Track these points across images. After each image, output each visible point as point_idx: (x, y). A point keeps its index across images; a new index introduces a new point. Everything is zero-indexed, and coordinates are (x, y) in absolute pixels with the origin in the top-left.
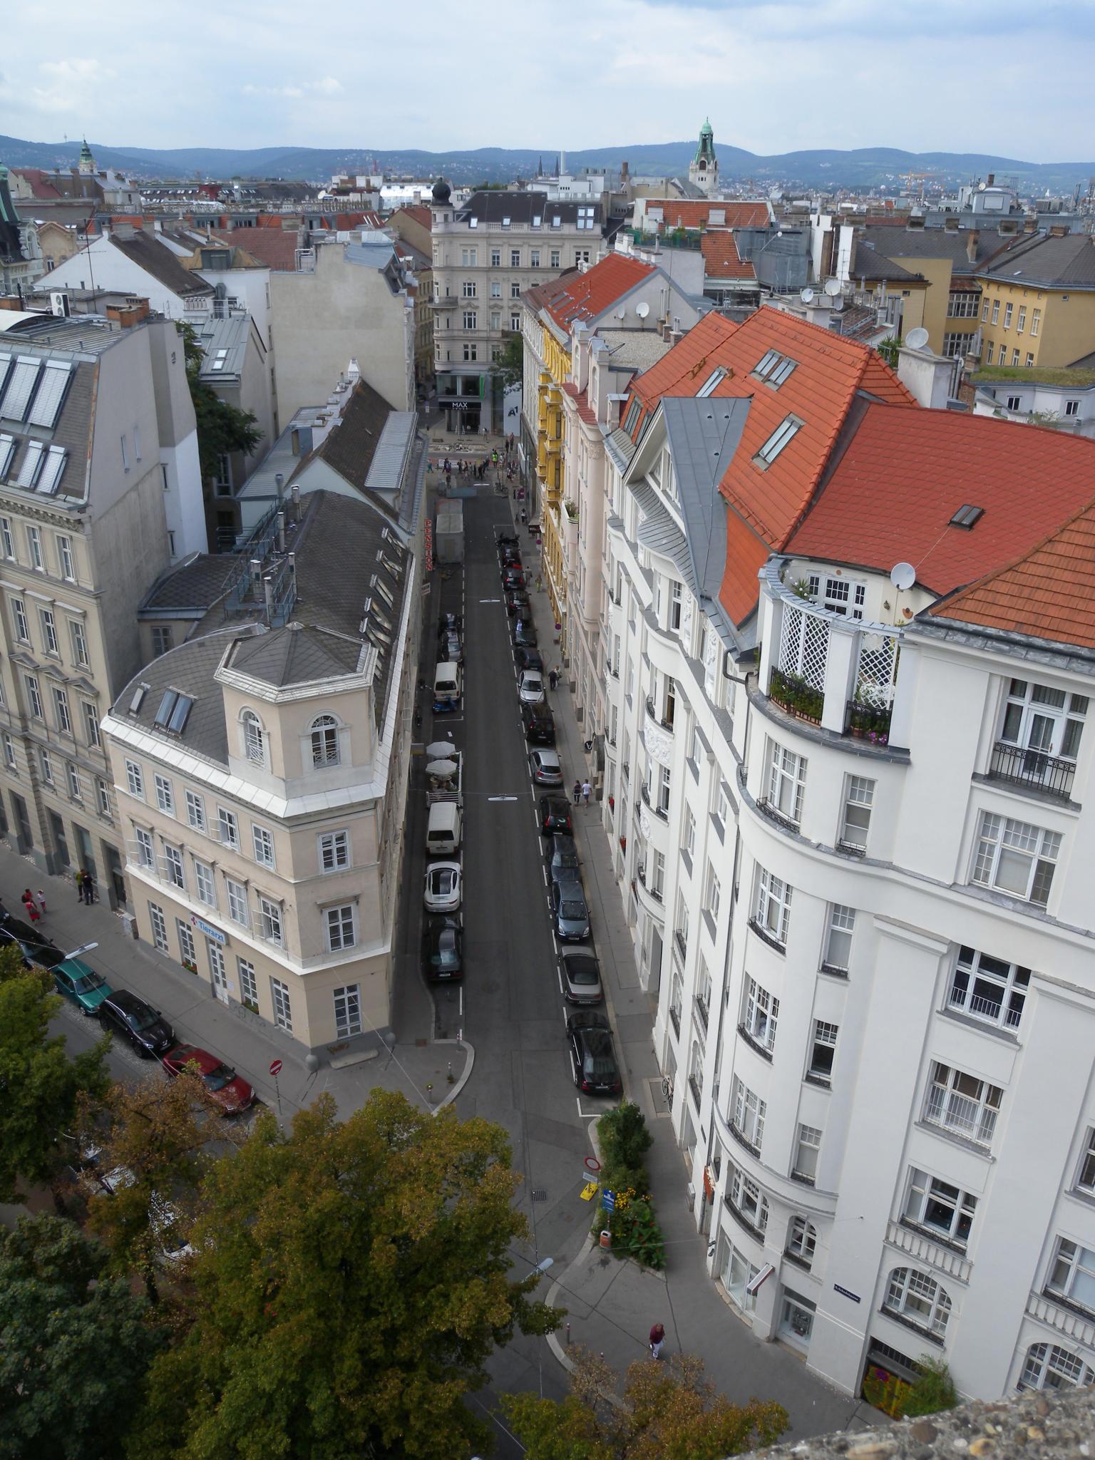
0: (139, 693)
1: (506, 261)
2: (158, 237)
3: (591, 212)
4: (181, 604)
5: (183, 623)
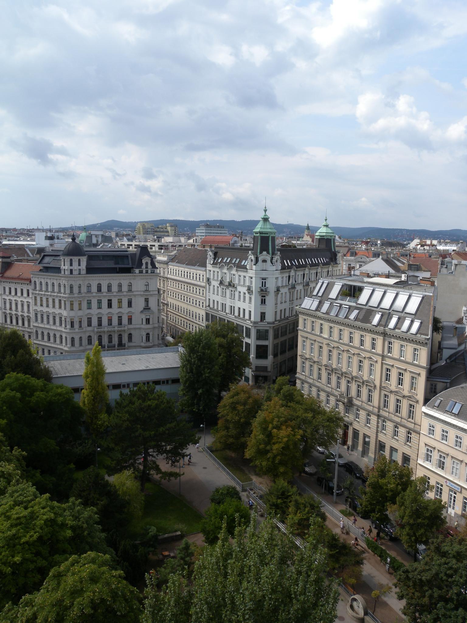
0: (439, 401)
2: (392, 259)
4: (442, 377)
5: (442, 383)
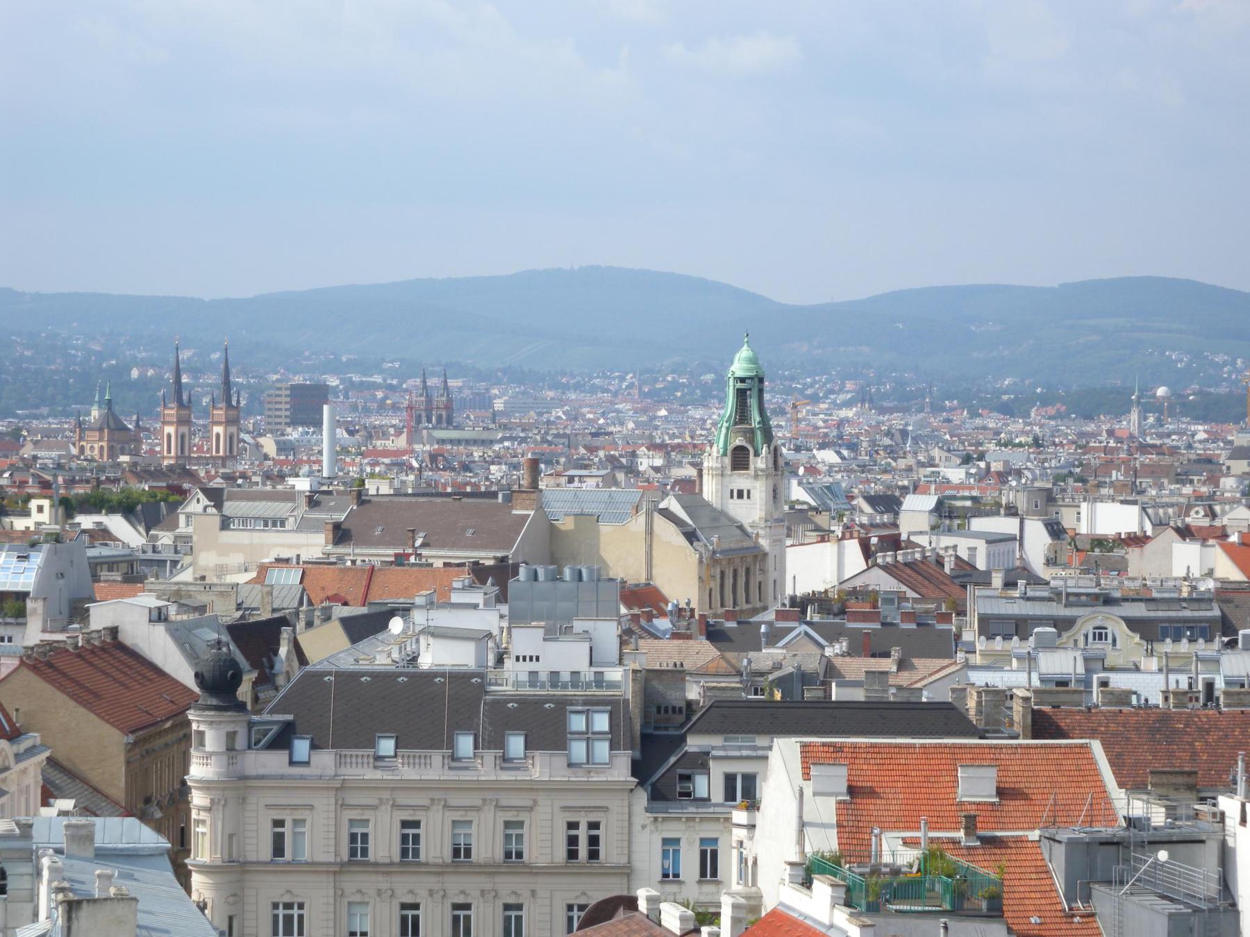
1: (384, 846)
3: (602, 722)
